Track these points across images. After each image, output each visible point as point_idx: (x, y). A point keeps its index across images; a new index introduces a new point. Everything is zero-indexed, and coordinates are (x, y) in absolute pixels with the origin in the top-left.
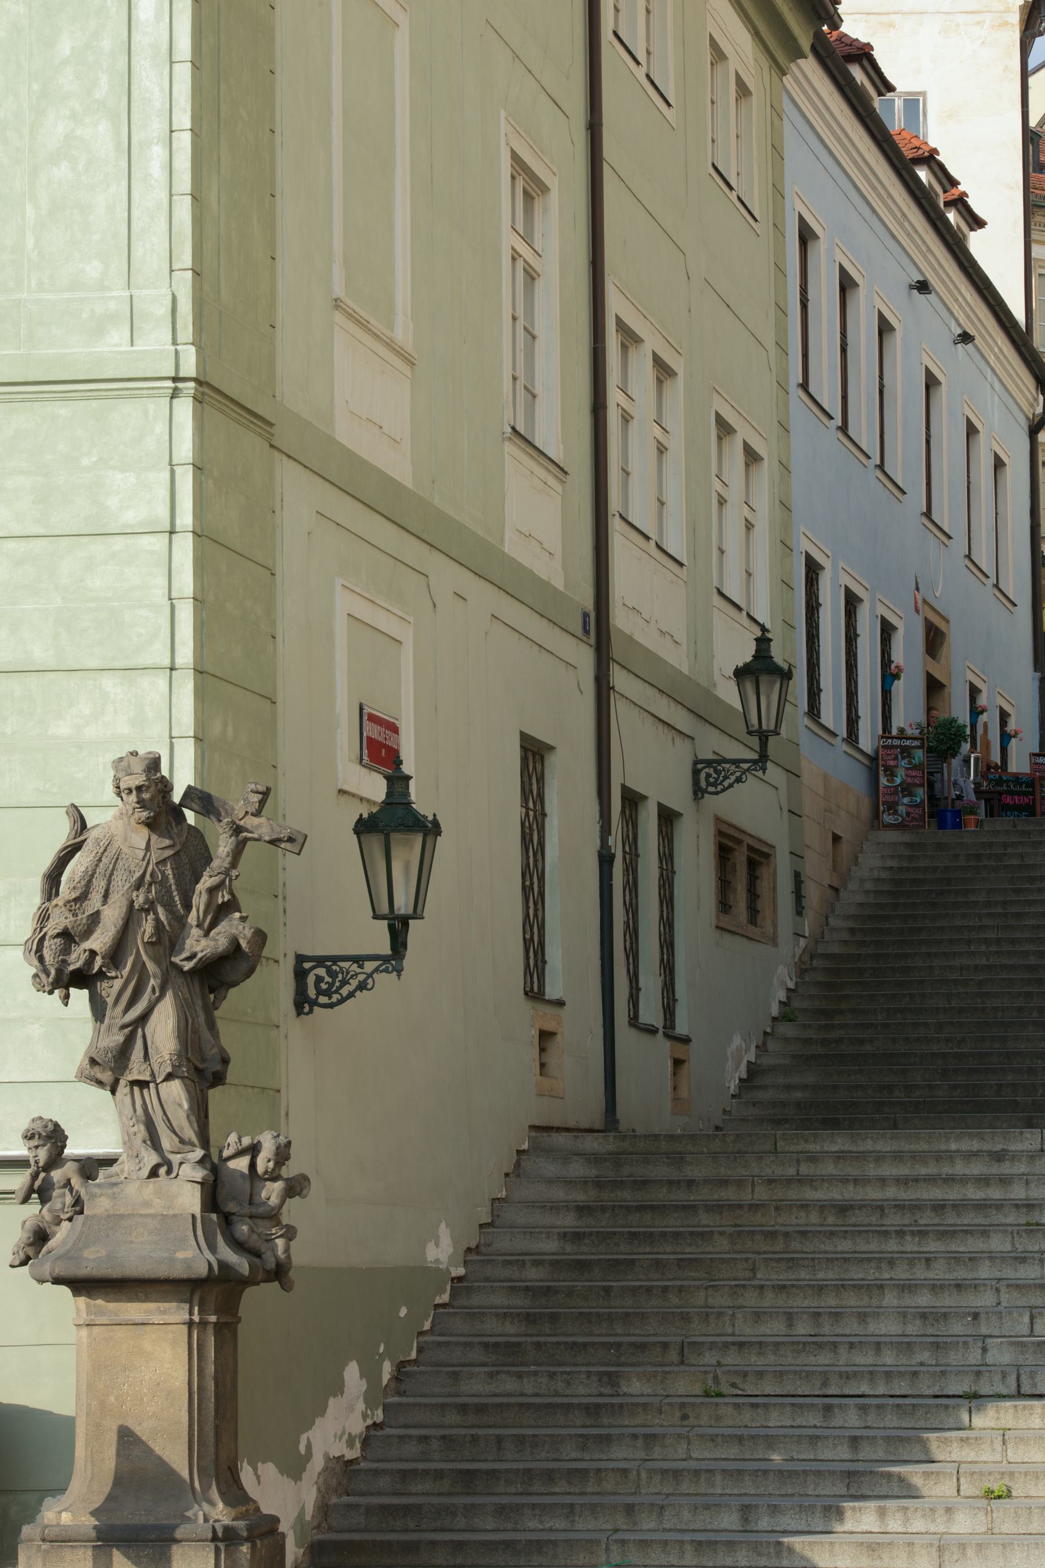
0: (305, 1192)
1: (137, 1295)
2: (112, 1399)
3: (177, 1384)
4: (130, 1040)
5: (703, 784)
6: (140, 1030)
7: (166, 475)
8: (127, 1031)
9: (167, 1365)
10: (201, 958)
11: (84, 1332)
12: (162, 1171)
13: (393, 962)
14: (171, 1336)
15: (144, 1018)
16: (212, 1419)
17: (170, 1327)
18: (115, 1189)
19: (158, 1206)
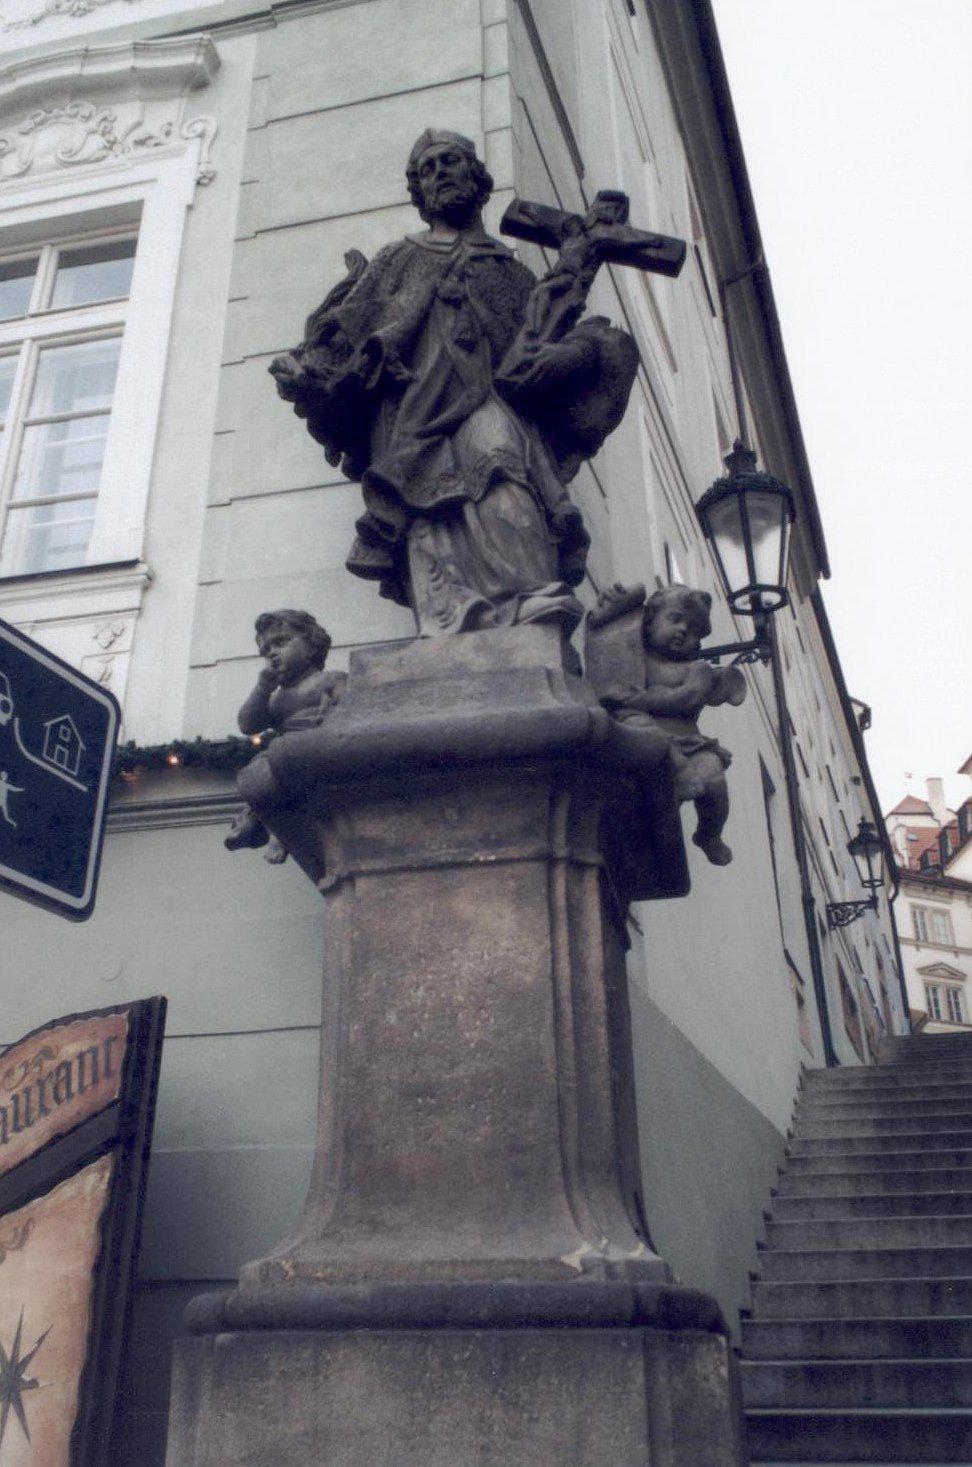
0: (737, 698)
1: (442, 812)
2: (392, 1018)
3: (529, 979)
4: (429, 452)
5: (834, 920)
6: (447, 444)
7: (477, 32)
8: (427, 442)
9: (505, 943)
10: (541, 368)
11: (338, 903)
12: (488, 616)
13: (757, 651)
14: (512, 884)
15: (452, 429)
16: (604, 1060)
17: (509, 870)
18: (403, 653)
19: (480, 663)
